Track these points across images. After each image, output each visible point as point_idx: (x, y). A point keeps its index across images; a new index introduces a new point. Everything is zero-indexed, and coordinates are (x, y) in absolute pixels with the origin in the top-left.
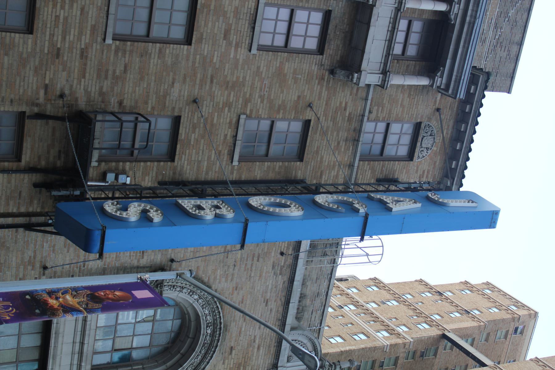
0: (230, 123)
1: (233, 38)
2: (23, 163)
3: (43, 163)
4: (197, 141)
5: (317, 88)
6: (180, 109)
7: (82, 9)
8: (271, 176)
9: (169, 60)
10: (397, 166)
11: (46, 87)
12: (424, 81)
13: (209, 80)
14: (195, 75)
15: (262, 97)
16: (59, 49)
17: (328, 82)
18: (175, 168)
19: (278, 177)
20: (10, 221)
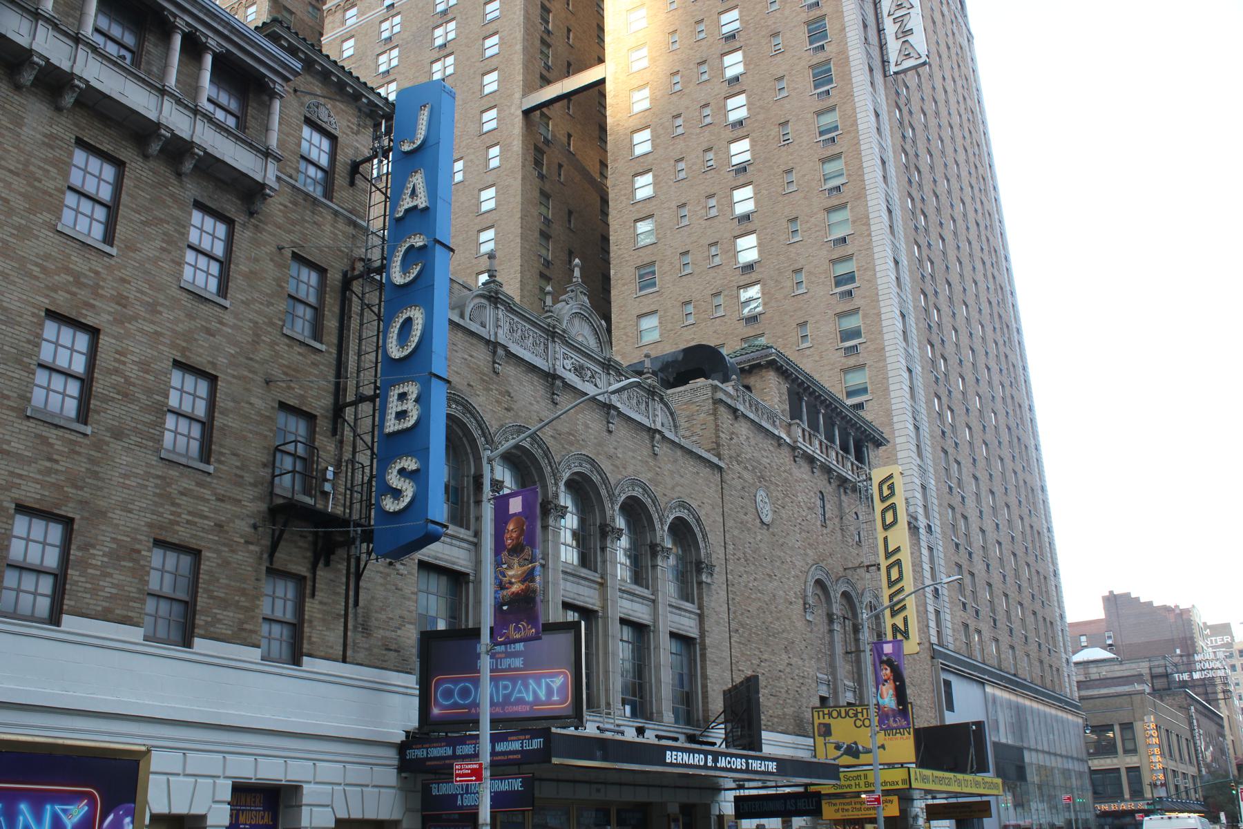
0: (288, 346)
1: (214, 325)
2: (308, 574)
3: (309, 554)
4: (301, 387)
5: (265, 236)
6: (274, 400)
7: (182, 494)
8: (336, 309)
9: (231, 405)
10: (340, 157)
11: (247, 542)
12: (277, 104)
13: (250, 362)
14: (245, 377)
15: (270, 304)
16: (216, 525)
17: (260, 221)
18: (322, 415)
19: (338, 302)
20: (352, 593)
